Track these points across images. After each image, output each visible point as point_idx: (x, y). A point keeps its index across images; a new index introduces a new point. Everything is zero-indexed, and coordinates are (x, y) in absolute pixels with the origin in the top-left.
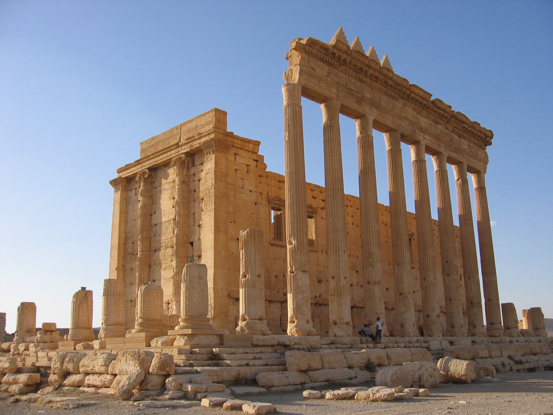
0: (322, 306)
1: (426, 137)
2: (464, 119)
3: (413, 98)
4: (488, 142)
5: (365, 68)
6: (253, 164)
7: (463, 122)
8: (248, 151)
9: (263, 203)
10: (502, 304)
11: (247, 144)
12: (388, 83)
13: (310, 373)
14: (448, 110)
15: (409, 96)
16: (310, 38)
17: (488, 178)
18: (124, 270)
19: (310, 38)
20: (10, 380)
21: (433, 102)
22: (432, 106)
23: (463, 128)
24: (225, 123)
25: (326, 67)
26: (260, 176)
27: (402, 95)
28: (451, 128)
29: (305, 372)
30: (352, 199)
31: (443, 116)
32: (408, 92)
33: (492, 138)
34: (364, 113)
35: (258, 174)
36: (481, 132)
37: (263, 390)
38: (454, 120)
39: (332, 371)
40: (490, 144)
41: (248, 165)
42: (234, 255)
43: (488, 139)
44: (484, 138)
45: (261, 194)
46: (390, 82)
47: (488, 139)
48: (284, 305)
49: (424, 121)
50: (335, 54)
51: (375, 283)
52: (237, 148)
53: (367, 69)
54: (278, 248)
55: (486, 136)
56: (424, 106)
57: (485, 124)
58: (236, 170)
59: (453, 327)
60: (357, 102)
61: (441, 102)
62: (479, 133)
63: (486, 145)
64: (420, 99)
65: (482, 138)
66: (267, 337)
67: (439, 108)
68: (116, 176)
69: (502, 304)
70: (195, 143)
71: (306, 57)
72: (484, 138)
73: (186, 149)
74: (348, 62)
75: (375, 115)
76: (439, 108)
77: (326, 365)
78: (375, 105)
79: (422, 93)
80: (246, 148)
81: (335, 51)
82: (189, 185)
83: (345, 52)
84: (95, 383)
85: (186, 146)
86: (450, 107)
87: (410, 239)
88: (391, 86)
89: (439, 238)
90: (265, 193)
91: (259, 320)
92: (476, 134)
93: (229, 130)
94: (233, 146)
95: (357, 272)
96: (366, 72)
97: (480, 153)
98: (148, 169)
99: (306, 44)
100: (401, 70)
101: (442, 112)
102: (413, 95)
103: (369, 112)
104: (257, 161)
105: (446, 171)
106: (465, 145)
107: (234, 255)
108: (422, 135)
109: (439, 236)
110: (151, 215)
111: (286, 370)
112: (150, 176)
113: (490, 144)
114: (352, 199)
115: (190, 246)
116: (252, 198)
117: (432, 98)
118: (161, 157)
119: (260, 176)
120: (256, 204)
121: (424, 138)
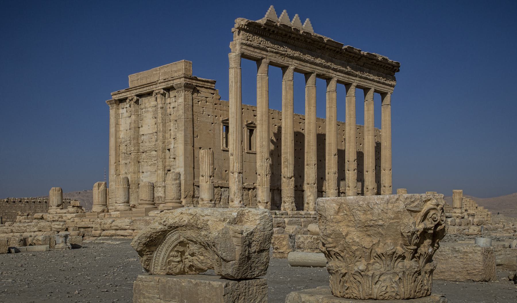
3: (328, 48)
4: (396, 70)
11: (206, 83)
12: (306, 41)
15: (324, 47)
40: (398, 71)
41: (207, 98)
43: (395, 68)
47: (395, 68)
55: (394, 66)
56: (338, 52)
63: (394, 72)
64: (334, 48)
65: (390, 68)
70: (169, 82)
73: (164, 85)
75: (296, 65)
85: (164, 84)
102: (327, 46)
113: (398, 71)
118: (145, 89)
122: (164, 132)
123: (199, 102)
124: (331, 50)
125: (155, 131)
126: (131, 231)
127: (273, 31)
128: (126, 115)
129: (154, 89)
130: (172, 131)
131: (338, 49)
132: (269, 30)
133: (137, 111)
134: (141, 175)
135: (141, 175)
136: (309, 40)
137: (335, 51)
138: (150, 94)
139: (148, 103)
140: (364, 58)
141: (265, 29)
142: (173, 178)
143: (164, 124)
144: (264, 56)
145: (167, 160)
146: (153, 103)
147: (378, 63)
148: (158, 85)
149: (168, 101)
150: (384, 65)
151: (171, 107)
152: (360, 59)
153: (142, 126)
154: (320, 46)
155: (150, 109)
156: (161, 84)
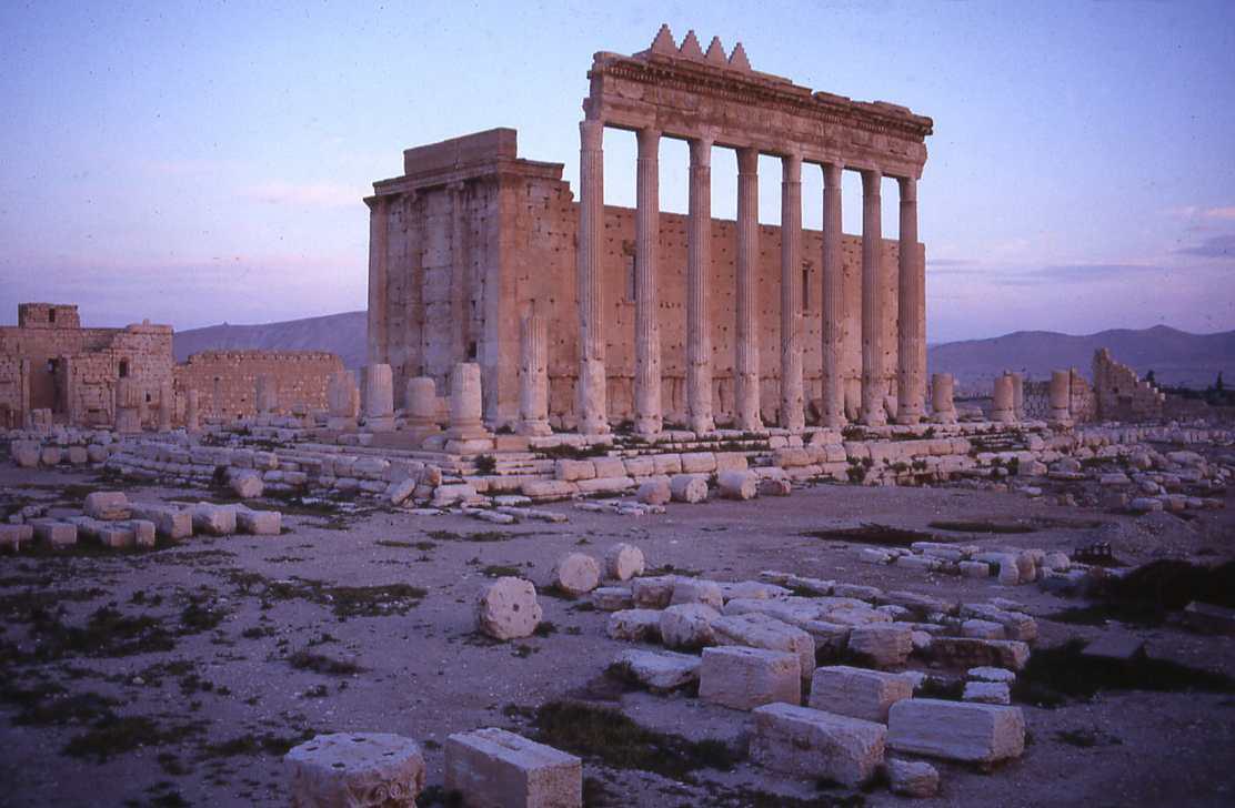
1: (805, 146)
5: (698, 77)
6: (553, 195)
8: (548, 179)
13: (580, 482)
15: (774, 97)
17: (923, 188)
18: (387, 325)
23: (876, 120)
25: (641, 86)
28: (855, 124)
29: (575, 481)
31: (837, 111)
32: (773, 93)
34: (698, 136)
36: (909, 121)
37: (528, 499)
38: (856, 112)
39: (607, 480)
40: (931, 133)
43: (924, 128)
45: (565, 235)
46: (741, 87)
47: (924, 128)
49: (801, 124)
52: (531, 177)
55: (921, 126)
57: (917, 109)
58: (530, 207)
61: (830, 95)
63: (923, 136)
64: (794, 98)
65: (912, 129)
66: (547, 438)
67: (828, 103)
68: (371, 193)
72: (919, 128)
73: (463, 175)
76: (828, 103)
77: (600, 475)
78: (711, 121)
79: (794, 90)
80: (544, 176)
81: (652, 66)
82: (468, 224)
84: (370, 489)
87: (805, 273)
89: (861, 265)
90: (570, 234)
91: (540, 419)
93: (519, 156)
94: (526, 176)
98: (417, 191)
100: (762, 62)
102: (779, 95)
104: (560, 190)
106: (881, 142)
109: (861, 260)
110: (421, 254)
111: (554, 479)
112: (419, 199)
113: (931, 133)
115: (471, 306)
116: (554, 242)
118: (432, 178)
120: (557, 250)
121: (801, 149)
122: (467, 266)
123: (530, 207)
125: (448, 263)
126: (382, 484)
128: (399, 226)
129: (449, 181)
130: (479, 265)
132: (659, 73)
133: (417, 221)
134: (425, 350)
135: (425, 350)
136: (741, 87)
137: (796, 101)
138: (441, 188)
139: (440, 206)
141: (650, 70)
143: (467, 250)
144: (649, 123)
145: (471, 323)
146: (447, 207)
147: (887, 120)
148: (456, 173)
149: (473, 205)
150: (899, 123)
151: (479, 216)
153: (426, 251)
155: (441, 219)
156: (461, 173)
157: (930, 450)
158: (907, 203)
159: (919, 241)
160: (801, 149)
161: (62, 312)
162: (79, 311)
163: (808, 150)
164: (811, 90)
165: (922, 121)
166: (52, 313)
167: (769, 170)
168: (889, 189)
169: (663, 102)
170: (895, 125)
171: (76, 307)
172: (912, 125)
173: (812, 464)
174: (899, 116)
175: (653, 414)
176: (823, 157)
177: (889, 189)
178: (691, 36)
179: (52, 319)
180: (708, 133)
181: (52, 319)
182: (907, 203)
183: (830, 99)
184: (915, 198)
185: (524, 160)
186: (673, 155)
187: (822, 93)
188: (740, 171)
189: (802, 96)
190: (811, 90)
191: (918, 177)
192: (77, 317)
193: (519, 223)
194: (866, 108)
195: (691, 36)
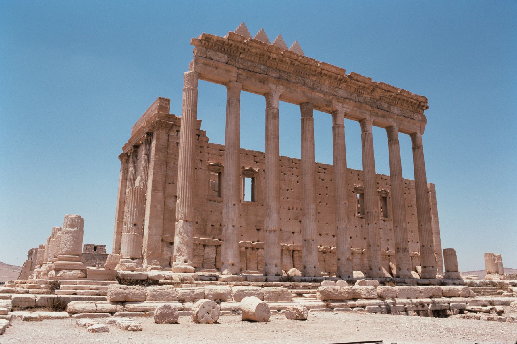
0: (260, 250)
1: (345, 106)
2: (389, 89)
3: (325, 75)
4: (423, 106)
7: (389, 91)
9: (203, 168)
10: (444, 250)
14: (367, 81)
16: (204, 34)
17: (425, 139)
19: (204, 34)
20: (37, 300)
21: (350, 77)
22: (349, 80)
24: (167, 109)
26: (201, 147)
27: (314, 73)
30: (297, 162)
33: (427, 103)
35: (200, 145)
40: (427, 108)
42: (171, 208)
43: (422, 104)
44: (419, 105)
46: (296, 63)
47: (422, 104)
48: (219, 249)
50: (231, 45)
51: (270, 231)
53: (269, 54)
54: (216, 203)
56: (341, 80)
59: (371, 269)
60: (261, 82)
62: (411, 100)
63: (423, 110)
65: (415, 104)
69: (444, 250)
71: (204, 49)
74: (246, 50)
79: (334, 70)
81: (231, 42)
83: (241, 42)
86: (370, 79)
88: (298, 65)
91: (132, 259)
92: (407, 101)
95: (300, 221)
96: (269, 57)
97: (416, 116)
99: (202, 39)
101: (363, 84)
102: (324, 72)
103: (275, 89)
105: (371, 134)
107: (171, 208)
108: (341, 105)
113: (427, 108)
114: (297, 162)
117: (348, 73)
119: (201, 147)
121: (343, 107)
124: (330, 77)
127: (244, 50)
131: (339, 76)
140: (378, 90)
142: (69, 223)
152: (373, 91)
154: (315, 71)
157: (443, 293)
158: (417, 147)
159: (429, 181)
160: (343, 107)
161: (99, 247)
162: (106, 248)
163: (348, 108)
164: (344, 71)
165: (422, 100)
166: (95, 248)
167: (322, 120)
168: (405, 141)
169: (241, 66)
170: (403, 100)
171: (105, 246)
172: (414, 101)
173: (350, 300)
174: (405, 94)
175: (230, 262)
176: (358, 113)
177: (405, 141)
178: (262, 32)
179: (95, 250)
180: (277, 90)
181: (95, 250)
182: (417, 147)
183: (359, 79)
184: (422, 142)
185: (174, 116)
186: (252, 105)
187: (353, 73)
188: (302, 116)
189: (339, 74)
190: (344, 71)
191: (422, 132)
192: (105, 250)
193: (169, 151)
194: (383, 87)
195: (262, 32)
